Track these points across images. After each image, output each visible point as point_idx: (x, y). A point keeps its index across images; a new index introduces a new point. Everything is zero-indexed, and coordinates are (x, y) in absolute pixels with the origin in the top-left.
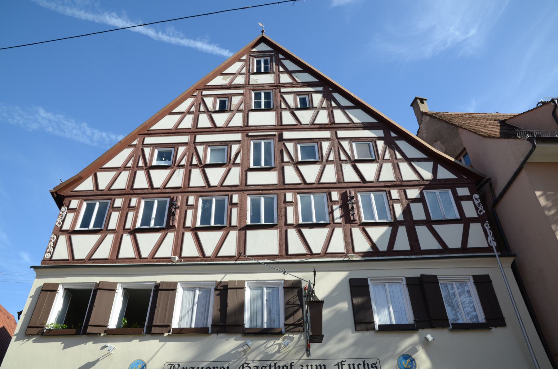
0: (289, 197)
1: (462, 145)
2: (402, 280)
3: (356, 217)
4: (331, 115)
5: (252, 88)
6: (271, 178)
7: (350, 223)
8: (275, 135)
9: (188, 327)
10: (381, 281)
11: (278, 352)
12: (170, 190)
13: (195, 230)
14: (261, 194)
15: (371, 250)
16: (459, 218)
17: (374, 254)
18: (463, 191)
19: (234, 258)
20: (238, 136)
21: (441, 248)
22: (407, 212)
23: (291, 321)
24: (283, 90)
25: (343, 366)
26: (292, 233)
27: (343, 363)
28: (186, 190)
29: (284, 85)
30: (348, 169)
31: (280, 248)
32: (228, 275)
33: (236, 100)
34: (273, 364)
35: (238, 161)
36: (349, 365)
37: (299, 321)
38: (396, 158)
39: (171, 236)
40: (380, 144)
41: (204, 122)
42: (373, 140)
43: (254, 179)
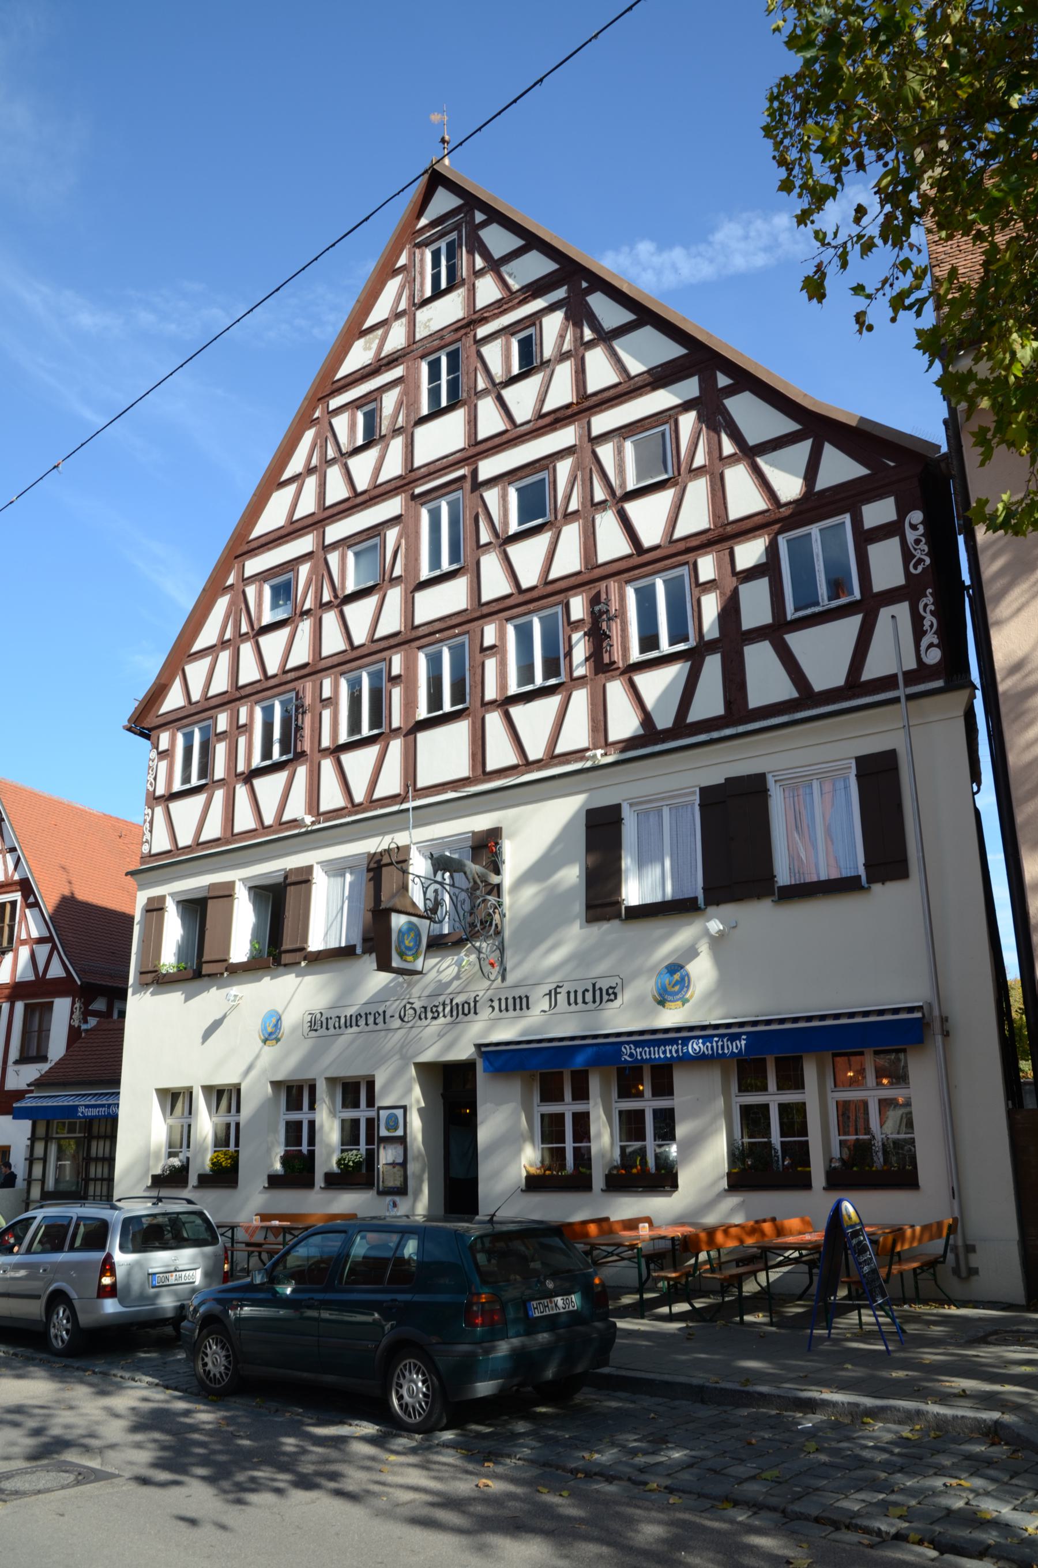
3: (617, 656)
5: (419, 352)
7: (604, 672)
9: (337, 946)
11: (457, 977)
13: (338, 750)
14: (441, 641)
18: (879, 512)
19: (398, 799)
22: (730, 611)
27: (559, 990)
28: (315, 669)
31: (473, 760)
36: (569, 993)
42: (669, 416)
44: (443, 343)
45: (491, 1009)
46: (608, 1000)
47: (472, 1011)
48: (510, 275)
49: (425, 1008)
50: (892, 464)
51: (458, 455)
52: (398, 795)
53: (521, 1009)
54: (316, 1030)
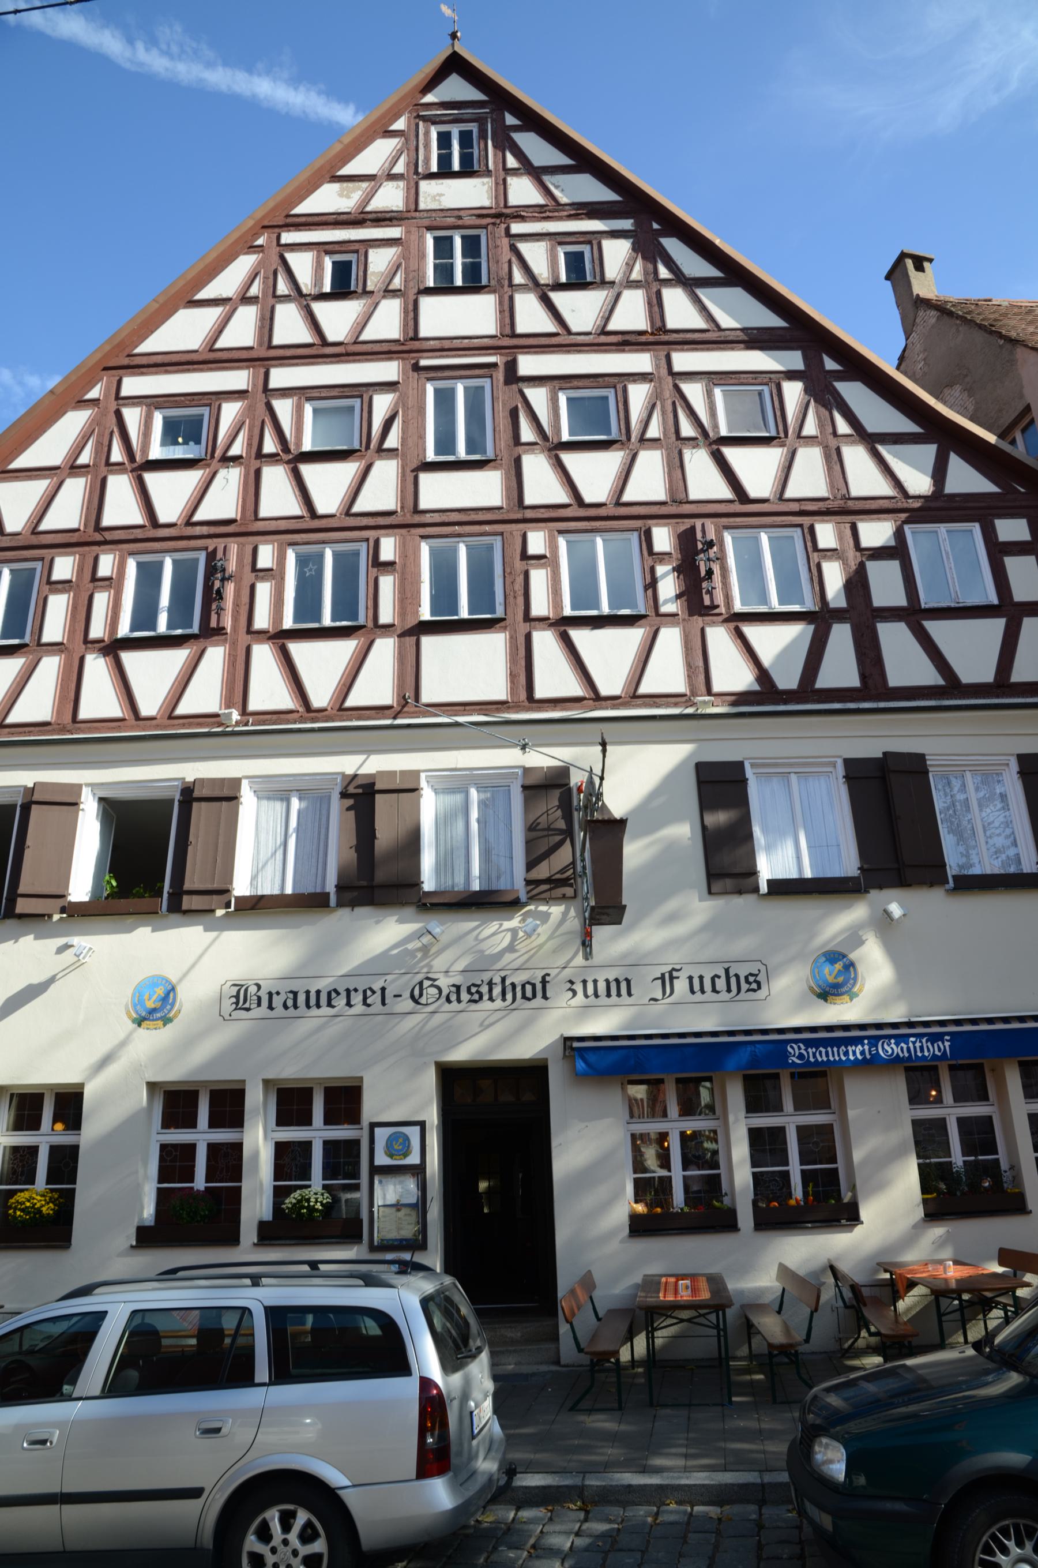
0: (537, 542)
1: (1021, 396)
2: (834, 765)
3: (719, 598)
4: (656, 306)
6: (483, 489)
7: (701, 615)
8: (495, 365)
9: (276, 891)
10: (779, 769)
11: (511, 948)
12: (205, 530)
13: (280, 638)
14: (459, 535)
15: (757, 688)
16: (996, 602)
17: (764, 696)
18: (1013, 529)
19: (387, 712)
20: (388, 370)
21: (941, 682)
22: (857, 584)
23: (543, 871)
24: (516, 228)
25: (675, 981)
26: (545, 642)
27: (675, 974)
28: (248, 527)
29: (520, 214)
30: (699, 464)
31: (512, 682)
32: (373, 757)
33: (380, 261)
34: (497, 980)
35: (392, 441)
36: (691, 978)
37: (563, 871)
38: (835, 433)
39: (215, 657)
40: (793, 392)
41: (290, 327)
42: (773, 380)
43: (440, 492)
44: (460, 223)
45: (570, 994)
46: (748, 990)
47: (539, 994)
48: (557, 187)
49: (458, 988)
50: (1022, 490)
51: (486, 340)
52: (389, 708)
53: (619, 995)
54: (248, 1010)
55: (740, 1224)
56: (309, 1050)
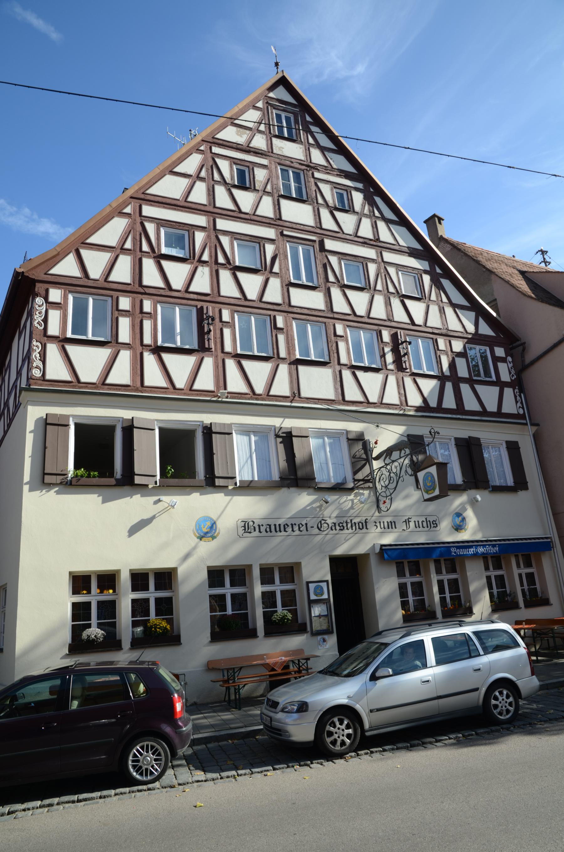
0: (340, 329)
1: (493, 295)
2: (450, 439)
7: (402, 372)
8: (315, 241)
11: (352, 508)
12: (195, 297)
14: (308, 320)
15: (423, 405)
16: (495, 380)
17: (425, 408)
21: (481, 410)
22: (452, 366)
23: (360, 476)
24: (317, 175)
32: (287, 420)
34: (349, 521)
36: (415, 522)
37: (367, 476)
38: (442, 301)
39: (208, 363)
40: (427, 279)
44: (292, 165)
47: (365, 527)
48: (331, 159)
49: (335, 524)
52: (288, 397)
53: (392, 528)
54: (250, 533)
55: (258, 634)
56: (277, 551)
